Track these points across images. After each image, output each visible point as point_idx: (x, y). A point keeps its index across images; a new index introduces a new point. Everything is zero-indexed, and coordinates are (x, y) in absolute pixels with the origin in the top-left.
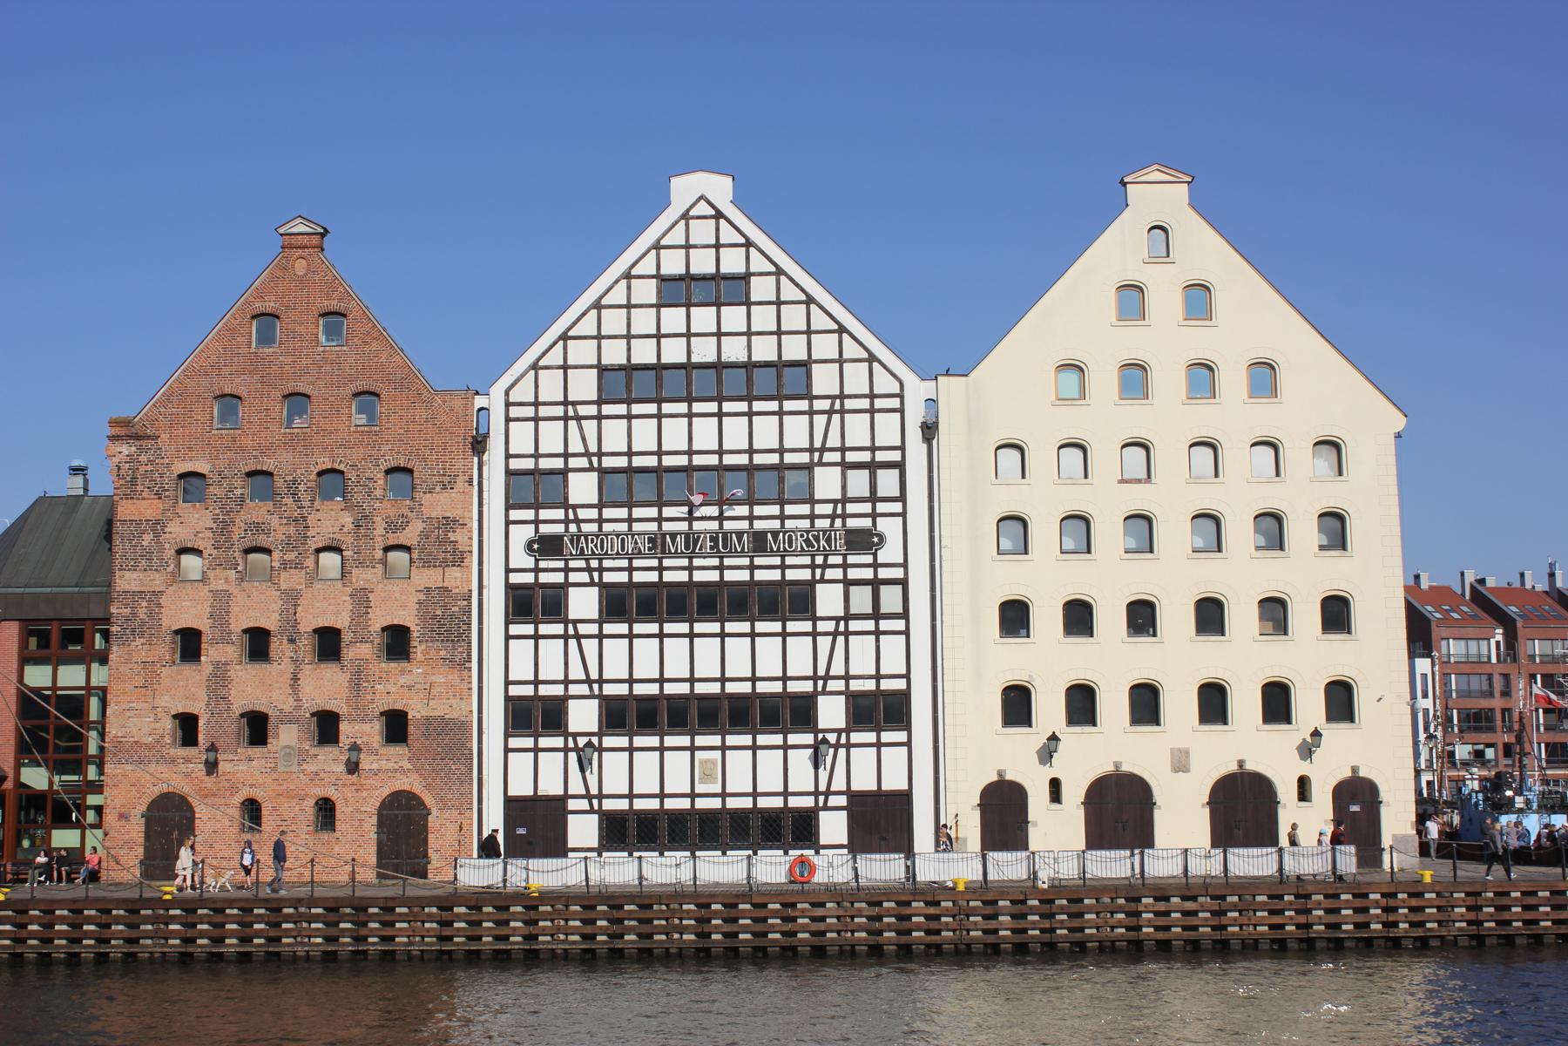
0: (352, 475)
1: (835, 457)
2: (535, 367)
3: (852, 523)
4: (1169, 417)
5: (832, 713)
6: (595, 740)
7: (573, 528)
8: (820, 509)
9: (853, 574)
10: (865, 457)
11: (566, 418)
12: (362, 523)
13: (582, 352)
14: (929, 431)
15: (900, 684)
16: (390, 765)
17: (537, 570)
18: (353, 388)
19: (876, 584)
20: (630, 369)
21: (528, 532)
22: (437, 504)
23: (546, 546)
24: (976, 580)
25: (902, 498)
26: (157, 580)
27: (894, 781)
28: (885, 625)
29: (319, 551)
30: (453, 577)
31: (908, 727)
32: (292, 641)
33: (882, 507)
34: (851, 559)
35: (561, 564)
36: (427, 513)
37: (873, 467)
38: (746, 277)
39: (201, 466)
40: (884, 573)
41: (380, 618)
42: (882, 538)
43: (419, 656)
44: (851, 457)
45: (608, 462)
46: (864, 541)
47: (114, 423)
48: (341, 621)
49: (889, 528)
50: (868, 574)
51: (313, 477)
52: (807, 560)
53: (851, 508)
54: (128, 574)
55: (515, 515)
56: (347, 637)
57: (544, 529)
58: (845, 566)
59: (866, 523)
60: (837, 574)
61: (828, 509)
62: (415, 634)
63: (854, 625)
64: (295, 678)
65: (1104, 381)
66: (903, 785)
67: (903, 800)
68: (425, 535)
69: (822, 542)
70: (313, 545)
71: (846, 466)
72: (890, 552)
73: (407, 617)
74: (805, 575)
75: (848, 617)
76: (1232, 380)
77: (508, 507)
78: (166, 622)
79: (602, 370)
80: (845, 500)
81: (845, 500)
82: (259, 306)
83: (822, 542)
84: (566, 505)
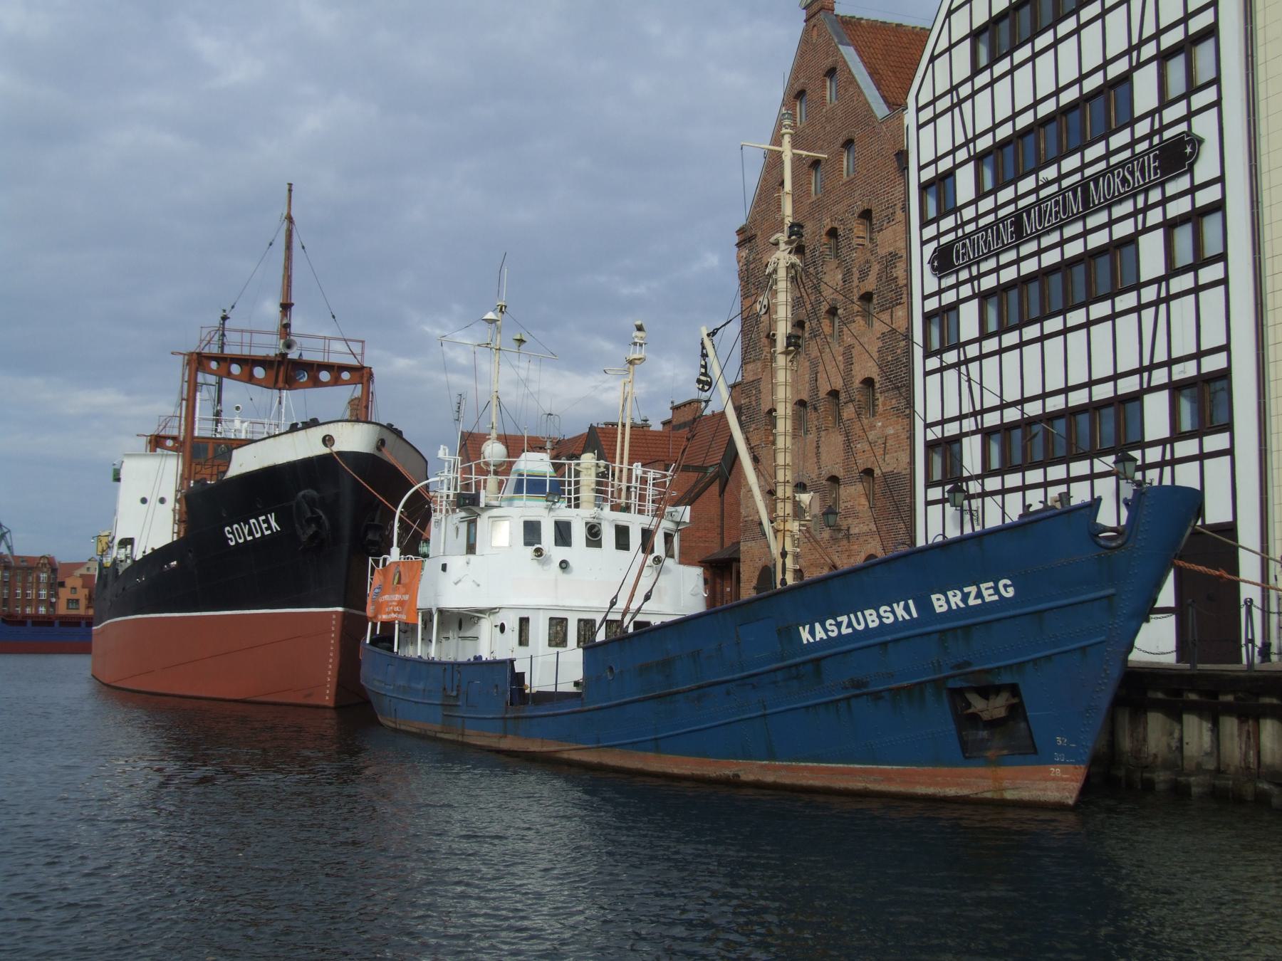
0: (840, 232)
1: (1149, 50)
2: (932, 59)
3: (1167, 134)
5: (1156, 416)
6: (974, 487)
7: (960, 233)
8: (1142, 128)
9: (1175, 209)
11: (951, 109)
12: (847, 275)
13: (961, 25)
16: (865, 529)
17: (940, 292)
18: (841, 140)
19: (1196, 217)
21: (934, 244)
22: (887, 240)
23: (944, 261)
25: (1216, 81)
26: (759, 364)
28: (1207, 274)
30: (900, 312)
31: (1228, 427)
32: (816, 409)
33: (1199, 100)
34: (1172, 189)
35: (951, 280)
36: (882, 251)
40: (1204, 198)
41: (859, 373)
42: (1197, 142)
43: (880, 409)
44: (1168, 40)
46: (1177, 156)
47: (741, 231)
48: (838, 384)
49: (1204, 126)
50: (1183, 206)
51: (825, 239)
52: (1127, 207)
53: (1170, 114)
54: (750, 367)
55: (930, 231)
56: (843, 397)
57: (944, 240)
58: (1164, 202)
59: (1183, 127)
60: (1155, 216)
61: (1142, 128)
62: (877, 385)
63: (1178, 284)
64: (818, 447)
66: (1229, 518)
68: (879, 278)
69: (1137, 174)
70: (825, 307)
72: (1205, 168)
73: (873, 371)
75: (1172, 271)
78: (763, 406)
79: (975, 35)
80: (1165, 103)
81: (1165, 103)
82: (797, 87)
83: (1137, 174)
84: (957, 210)
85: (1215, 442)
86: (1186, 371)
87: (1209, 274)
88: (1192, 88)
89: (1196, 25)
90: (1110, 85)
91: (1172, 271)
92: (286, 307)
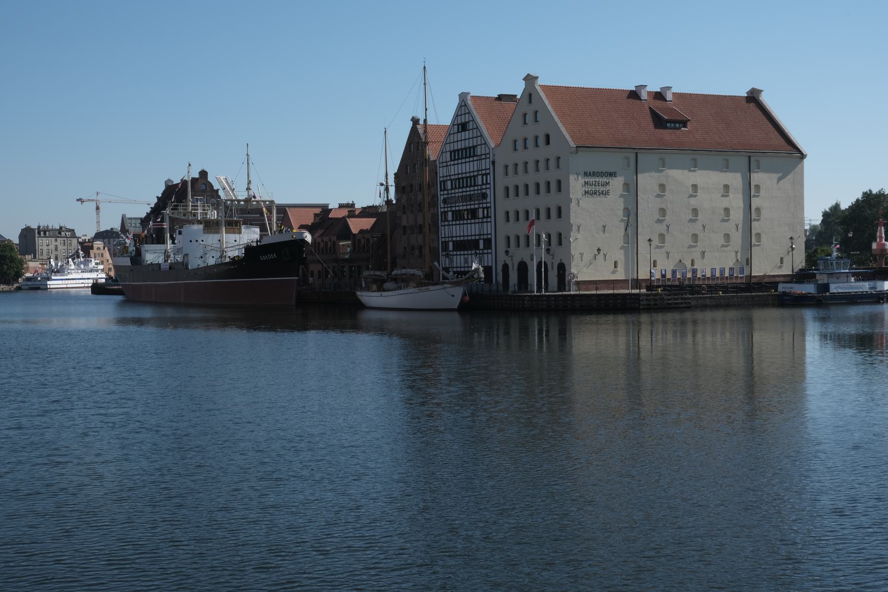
4: (531, 155)
10: (484, 172)
14: (493, 163)
15: (489, 236)
20: (454, 151)
24: (504, 205)
27: (490, 264)
29: (420, 205)
33: (488, 186)
37: (486, 174)
38: (468, 122)
39: (404, 184)
40: (489, 205)
45: (453, 177)
46: (484, 196)
49: (488, 191)
50: (485, 205)
53: (484, 187)
63: (485, 220)
65: (520, 145)
67: (491, 268)
71: (482, 175)
72: (488, 200)
74: (477, 206)
75: (484, 217)
76: (542, 141)
77: (441, 190)
81: (483, 184)
85: (489, 251)
86: (485, 237)
87: (489, 220)
88: (487, 183)
89: (488, 171)
90: (475, 176)
91: (484, 217)
92: (249, 182)
